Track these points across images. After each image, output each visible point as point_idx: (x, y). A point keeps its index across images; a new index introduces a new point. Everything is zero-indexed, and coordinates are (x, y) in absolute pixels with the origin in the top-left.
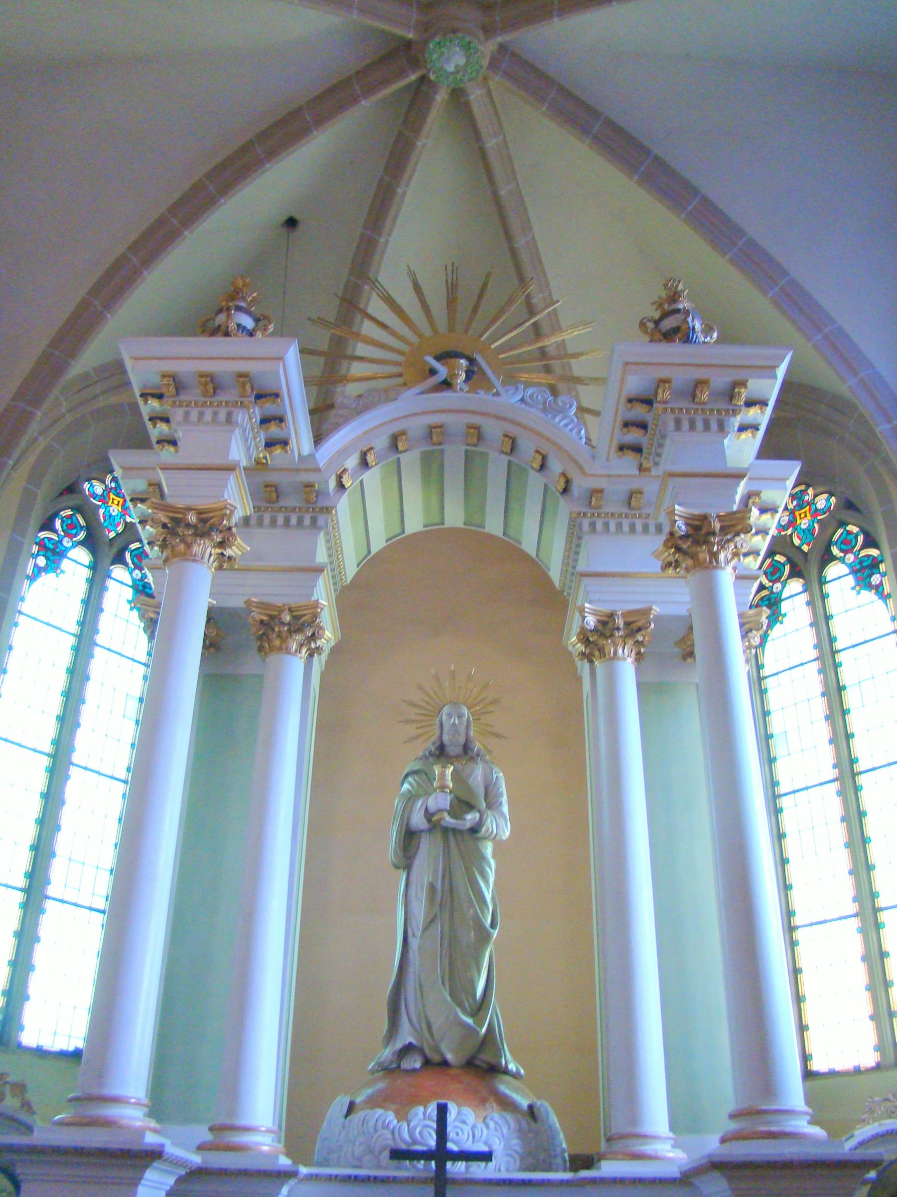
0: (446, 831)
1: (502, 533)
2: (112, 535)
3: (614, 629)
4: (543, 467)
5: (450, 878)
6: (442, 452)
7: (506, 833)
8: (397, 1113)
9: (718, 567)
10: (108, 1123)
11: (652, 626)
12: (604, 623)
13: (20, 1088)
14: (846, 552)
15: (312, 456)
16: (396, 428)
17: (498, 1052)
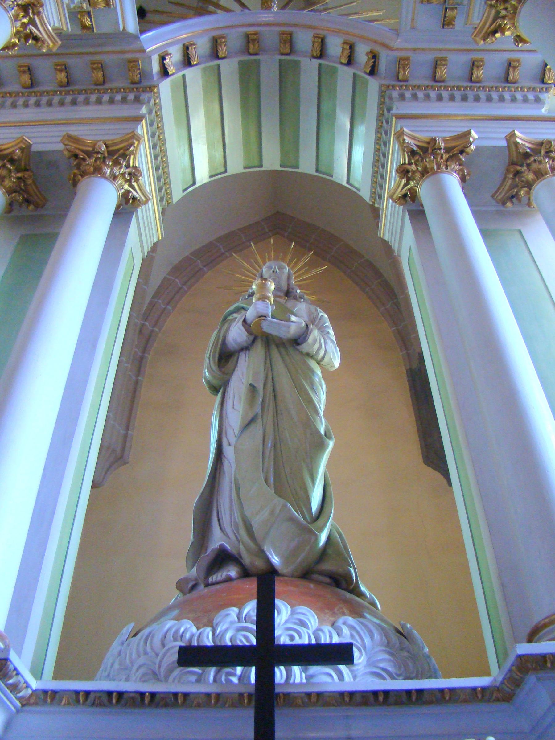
1: (315, 170)
3: (435, 149)
4: (350, 63)
5: (274, 386)
6: (258, 62)
7: (337, 363)
11: (473, 147)
12: (425, 150)
15: (136, 38)
16: (216, 33)
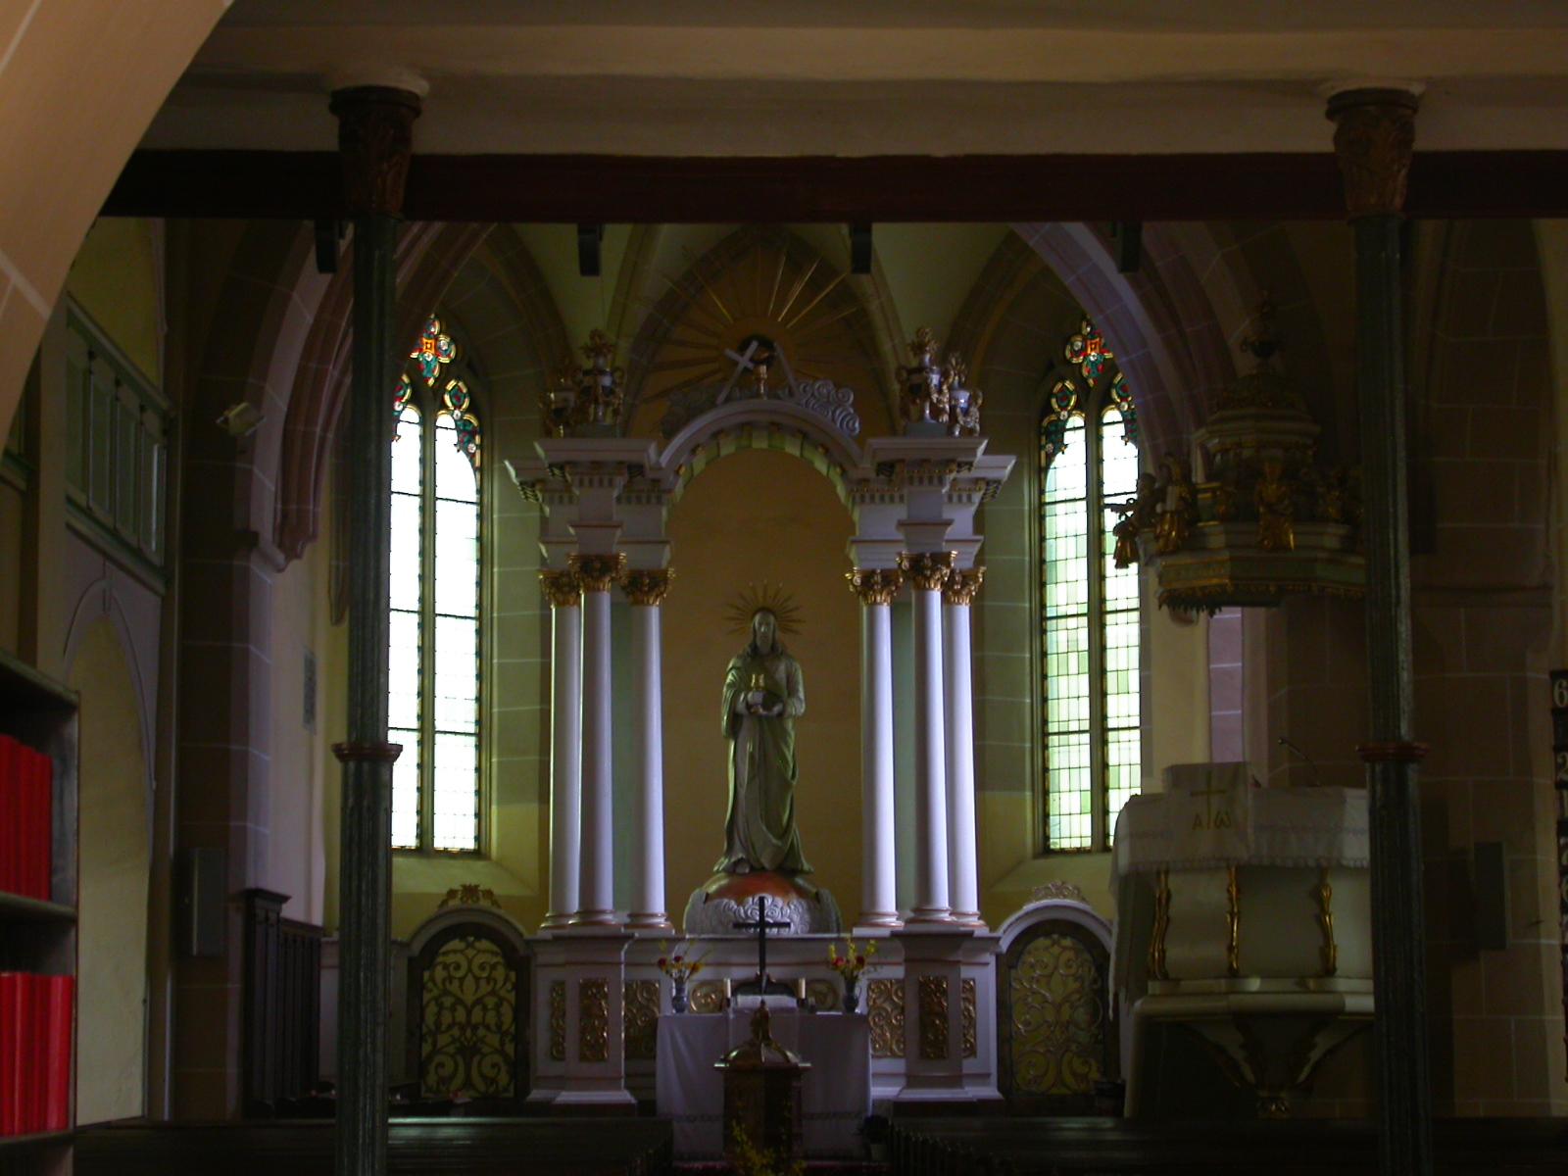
0: (760, 717)
2: (431, 382)
8: (736, 901)
9: (930, 589)
10: (601, 923)
13: (489, 894)
14: (1123, 399)
17: (797, 859)
